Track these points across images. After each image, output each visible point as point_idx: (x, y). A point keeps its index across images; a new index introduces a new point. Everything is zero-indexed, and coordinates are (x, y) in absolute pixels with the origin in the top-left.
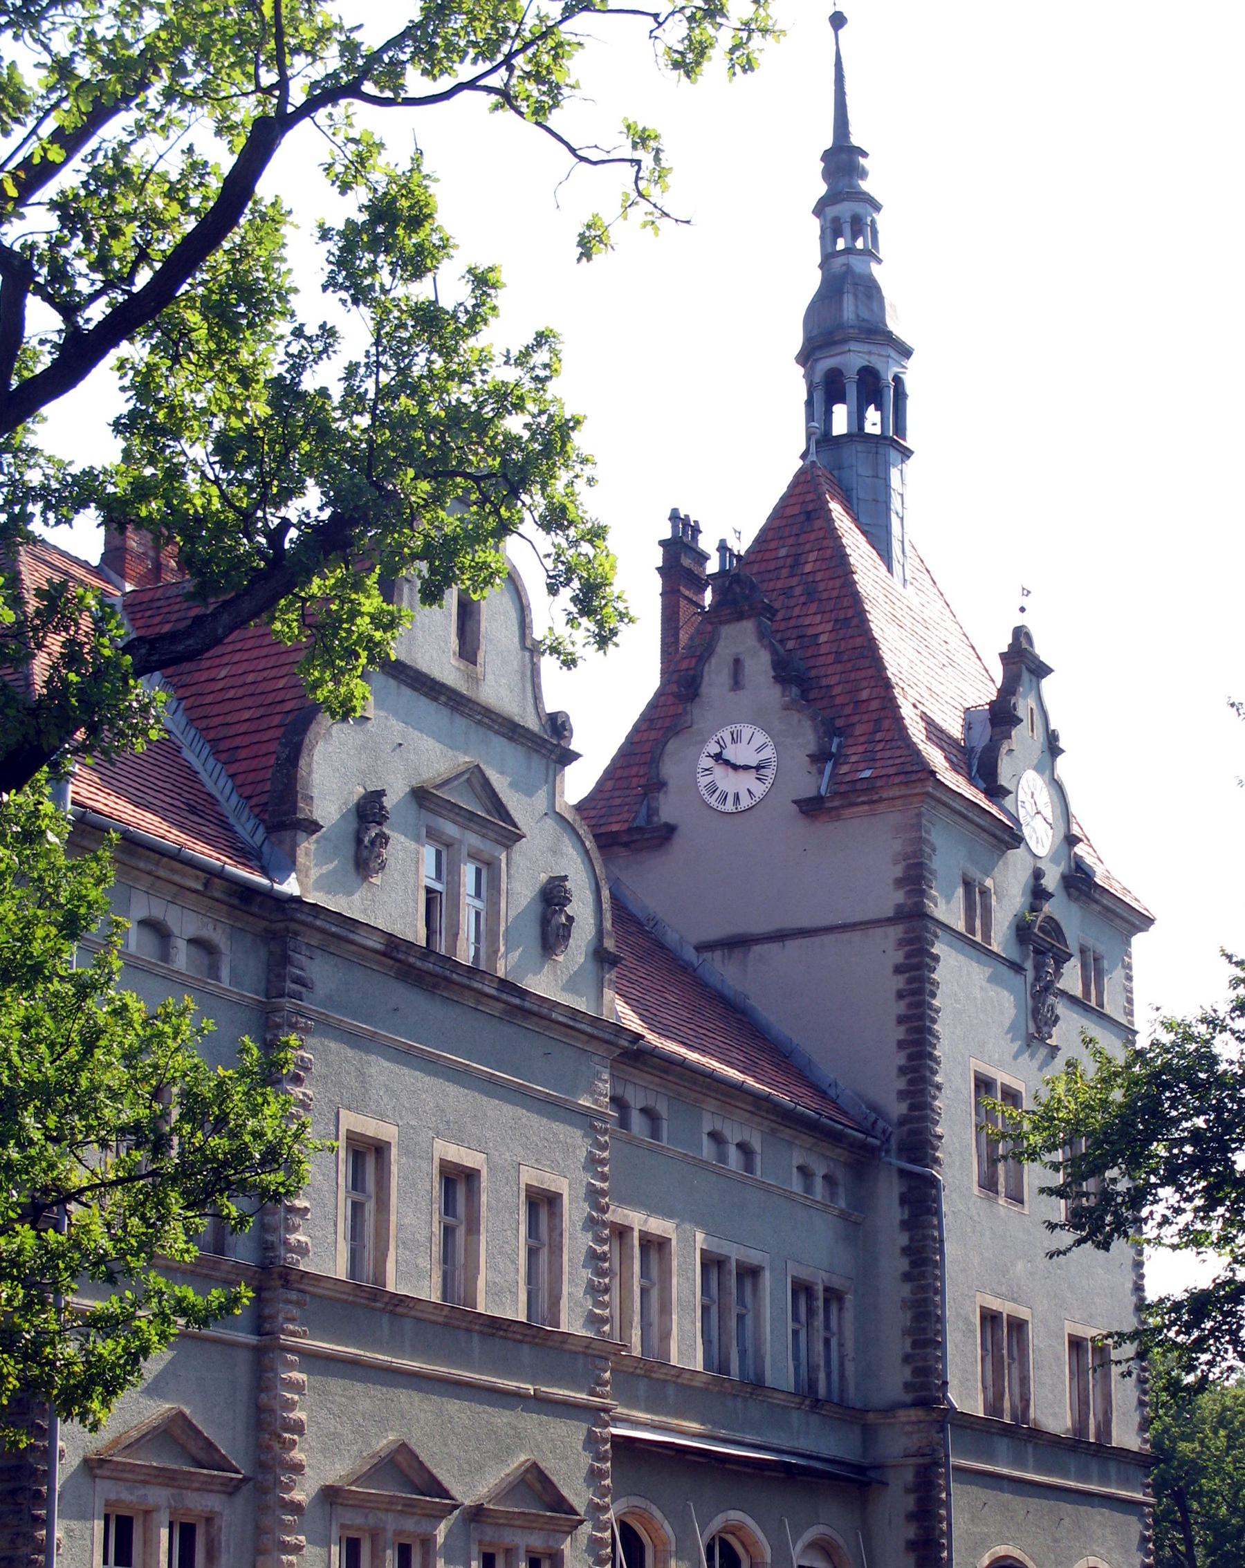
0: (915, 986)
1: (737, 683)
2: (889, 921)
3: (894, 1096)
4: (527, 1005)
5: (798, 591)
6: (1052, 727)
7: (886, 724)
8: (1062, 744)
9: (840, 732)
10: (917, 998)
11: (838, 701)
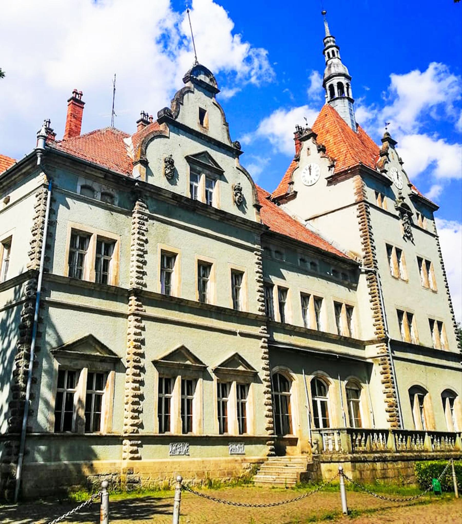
0: (363, 220)
1: (309, 155)
2: (355, 204)
3: (361, 250)
4: (227, 217)
5: (324, 132)
6: (400, 157)
7: (348, 156)
8: (403, 161)
9: (335, 160)
10: (364, 223)
11: (336, 153)
